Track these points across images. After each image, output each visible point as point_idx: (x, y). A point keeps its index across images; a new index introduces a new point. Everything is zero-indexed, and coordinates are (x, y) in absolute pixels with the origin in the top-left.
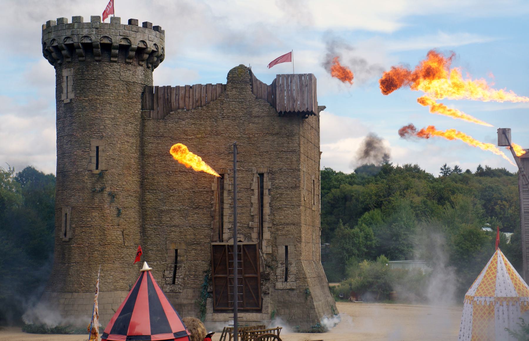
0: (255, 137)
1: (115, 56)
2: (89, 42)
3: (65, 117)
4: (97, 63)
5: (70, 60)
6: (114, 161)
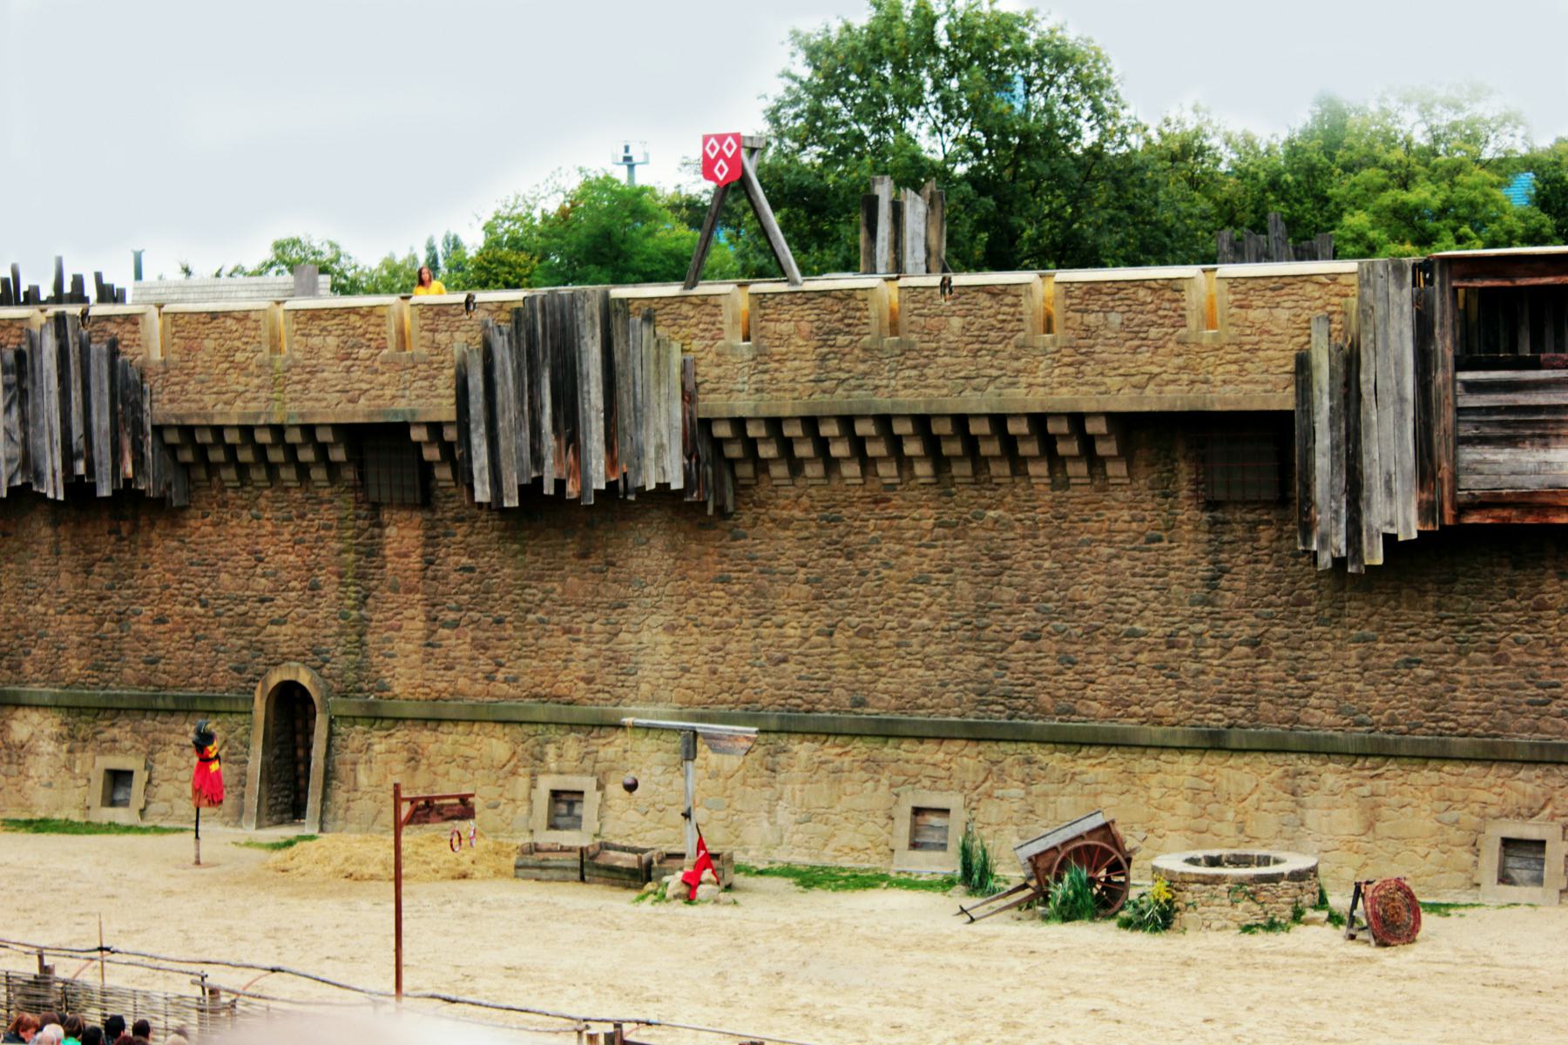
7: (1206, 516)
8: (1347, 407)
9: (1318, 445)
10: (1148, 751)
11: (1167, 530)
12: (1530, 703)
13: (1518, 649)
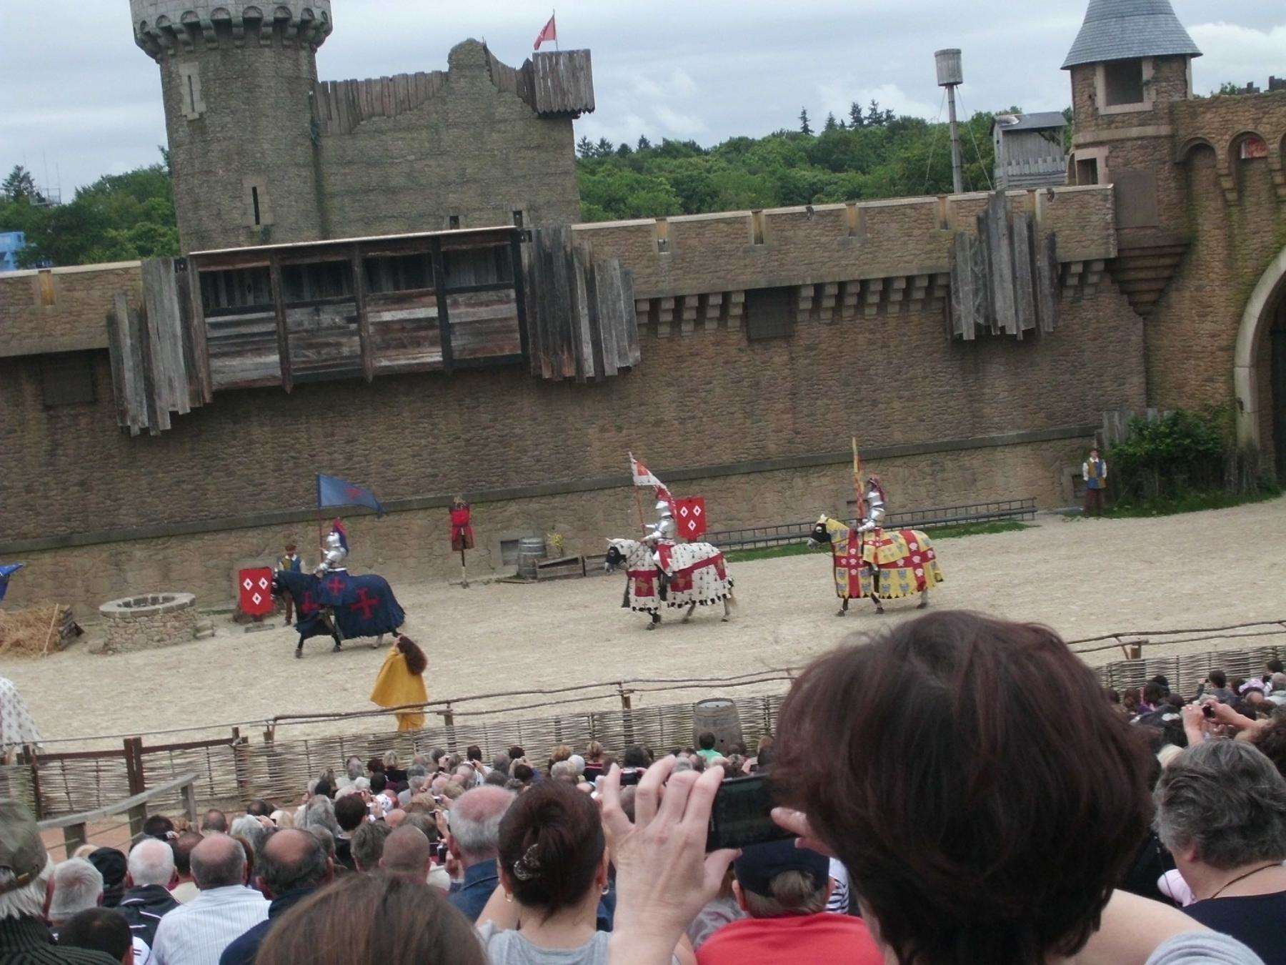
1: (266, 37)
2: (226, 17)
3: (191, 143)
5: (192, 48)
7: (44, 415)
8: (141, 342)
9: (126, 366)
10: (22, 555)
11: (20, 425)
12: (251, 496)
13: (241, 467)
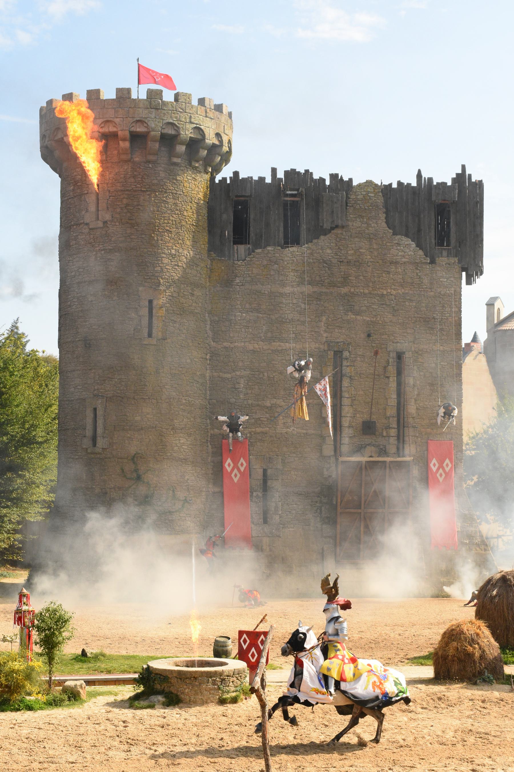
0: (392, 295)
4: (150, 166)
6: (175, 325)
